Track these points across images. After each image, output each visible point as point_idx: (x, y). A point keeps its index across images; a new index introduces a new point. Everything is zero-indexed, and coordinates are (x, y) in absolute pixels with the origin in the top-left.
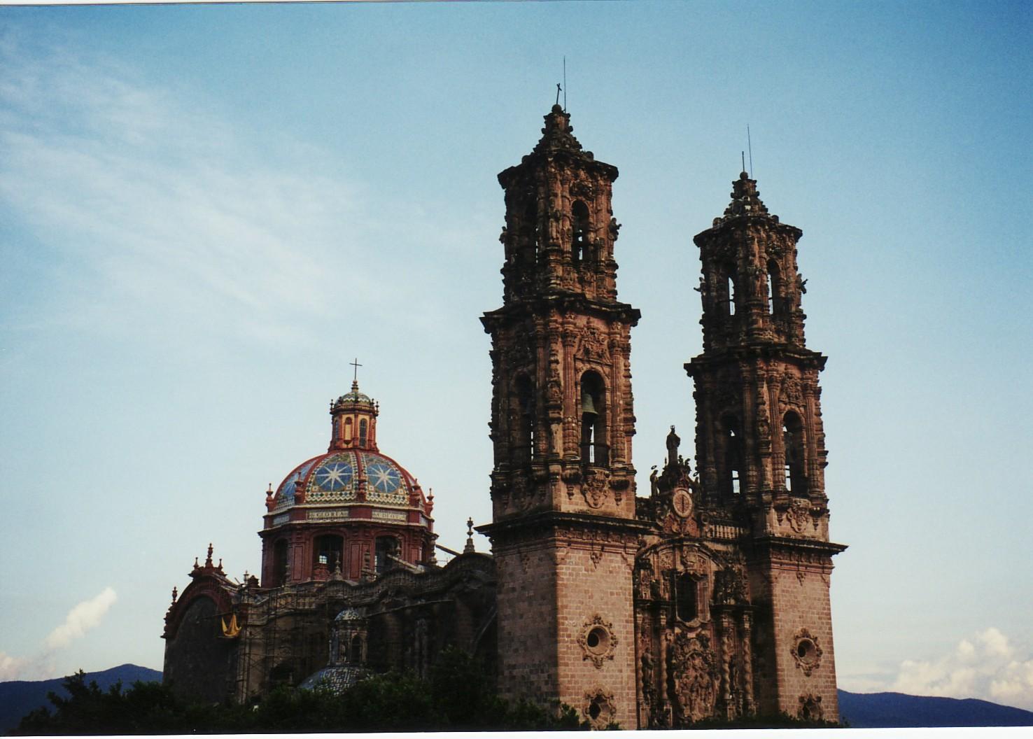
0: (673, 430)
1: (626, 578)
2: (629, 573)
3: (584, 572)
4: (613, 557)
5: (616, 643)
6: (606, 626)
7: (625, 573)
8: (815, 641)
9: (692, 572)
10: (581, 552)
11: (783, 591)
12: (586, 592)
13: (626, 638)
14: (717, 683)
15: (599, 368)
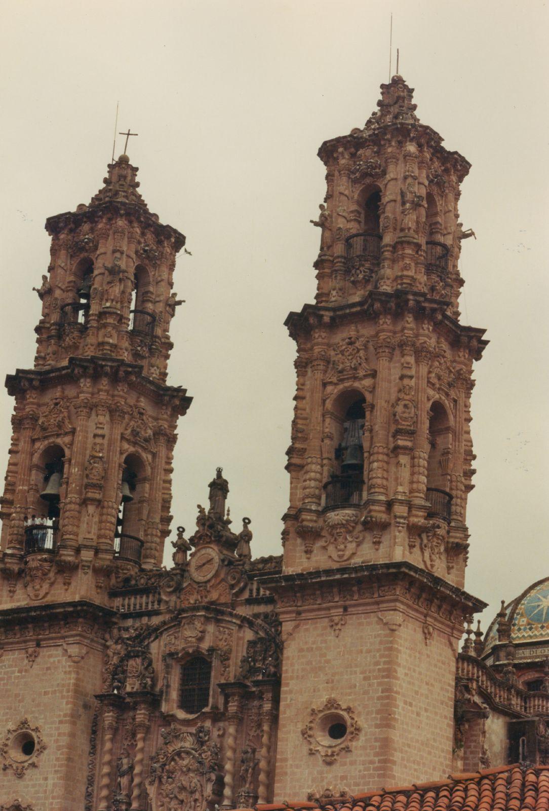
0: (219, 472)
1: (65, 672)
2: (70, 666)
3: (17, 674)
4: (53, 651)
5: (44, 748)
6: (33, 730)
7: (65, 667)
8: (348, 713)
9: (191, 651)
10: (17, 652)
11: (301, 650)
12: (17, 695)
13: (57, 741)
14: (209, 789)
15: (59, 441)
